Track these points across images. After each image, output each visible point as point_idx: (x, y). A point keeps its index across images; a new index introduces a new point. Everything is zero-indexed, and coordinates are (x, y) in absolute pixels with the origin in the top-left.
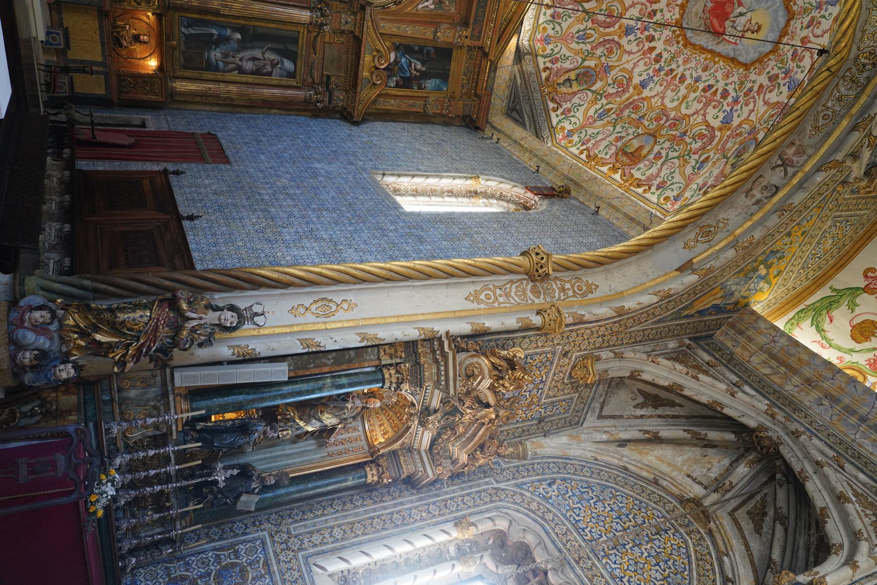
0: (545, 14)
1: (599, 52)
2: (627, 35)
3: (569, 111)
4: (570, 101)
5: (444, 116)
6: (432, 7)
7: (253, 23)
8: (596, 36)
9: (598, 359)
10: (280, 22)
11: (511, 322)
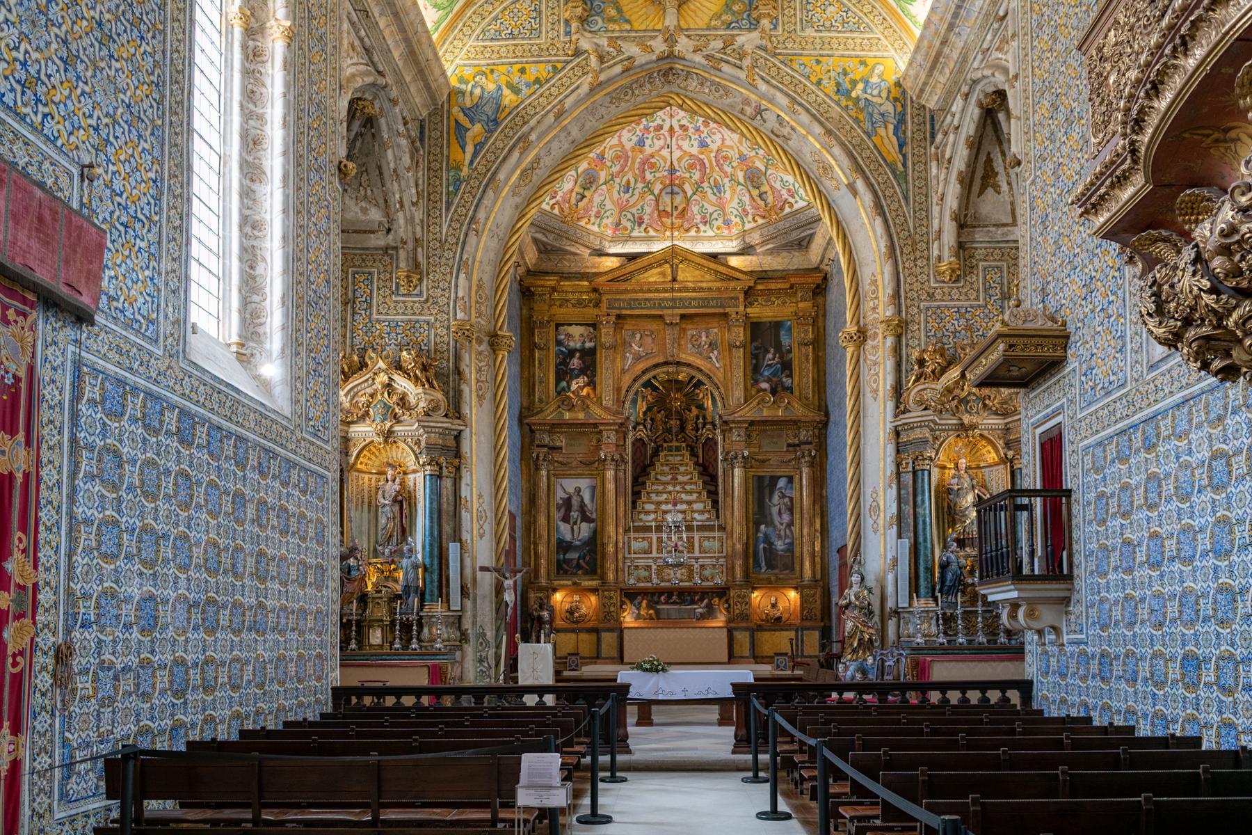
0: (705, 232)
1: (729, 170)
2: (708, 146)
3: (789, 190)
4: (779, 191)
5: (815, 320)
6: (716, 352)
7: (751, 515)
8: (715, 175)
10: (746, 493)
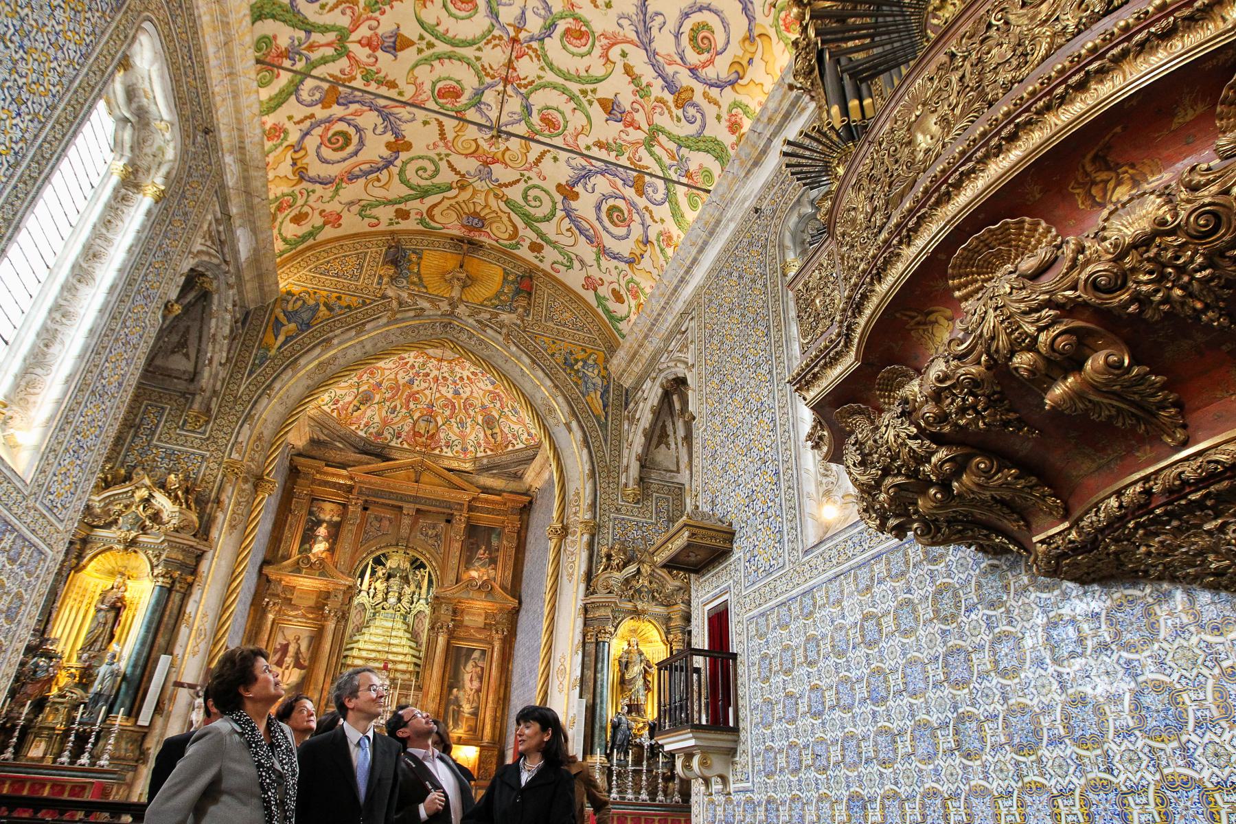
1: (472, 413)
9: (626, 485)
11: (585, 555)
